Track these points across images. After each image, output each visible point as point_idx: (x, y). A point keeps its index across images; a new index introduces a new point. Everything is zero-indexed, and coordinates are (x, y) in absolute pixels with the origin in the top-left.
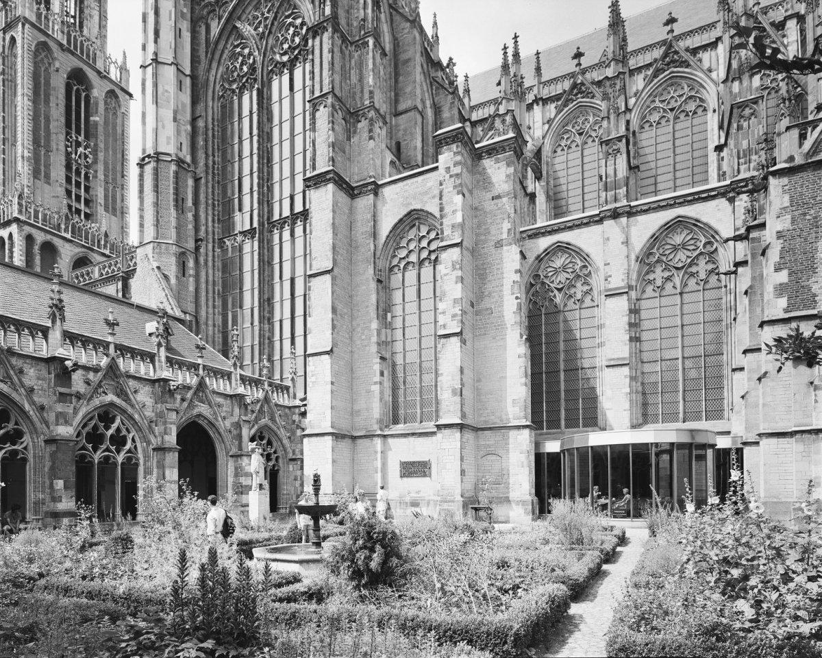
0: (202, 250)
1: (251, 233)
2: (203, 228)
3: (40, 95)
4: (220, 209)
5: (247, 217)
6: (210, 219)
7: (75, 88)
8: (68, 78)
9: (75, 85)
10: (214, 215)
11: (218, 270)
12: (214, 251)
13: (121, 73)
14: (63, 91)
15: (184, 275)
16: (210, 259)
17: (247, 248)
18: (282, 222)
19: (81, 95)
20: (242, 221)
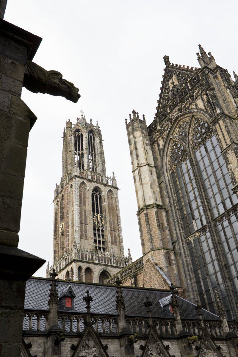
0: (177, 248)
1: (203, 230)
2: (175, 235)
3: (82, 203)
4: (182, 222)
5: (199, 221)
6: (178, 229)
7: (95, 195)
8: (93, 192)
9: (95, 193)
10: (179, 226)
11: (188, 257)
12: (183, 246)
13: (113, 181)
14: (91, 198)
15: (170, 265)
16: (182, 251)
17: (203, 238)
18: (221, 218)
19: (97, 196)
20: (197, 225)
